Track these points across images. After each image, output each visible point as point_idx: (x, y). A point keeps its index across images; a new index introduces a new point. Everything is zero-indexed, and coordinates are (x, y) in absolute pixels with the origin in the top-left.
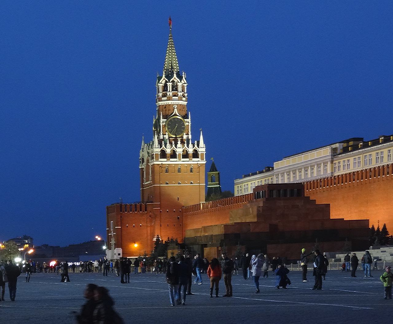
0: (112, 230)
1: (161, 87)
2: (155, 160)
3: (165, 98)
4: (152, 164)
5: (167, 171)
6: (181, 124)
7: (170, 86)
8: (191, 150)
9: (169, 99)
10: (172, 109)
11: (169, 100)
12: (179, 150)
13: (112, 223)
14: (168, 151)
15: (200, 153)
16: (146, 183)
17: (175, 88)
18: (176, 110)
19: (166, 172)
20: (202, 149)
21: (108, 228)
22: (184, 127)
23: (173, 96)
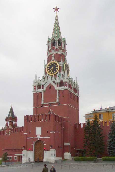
2: (67, 86)
3: (62, 50)
16: (44, 103)
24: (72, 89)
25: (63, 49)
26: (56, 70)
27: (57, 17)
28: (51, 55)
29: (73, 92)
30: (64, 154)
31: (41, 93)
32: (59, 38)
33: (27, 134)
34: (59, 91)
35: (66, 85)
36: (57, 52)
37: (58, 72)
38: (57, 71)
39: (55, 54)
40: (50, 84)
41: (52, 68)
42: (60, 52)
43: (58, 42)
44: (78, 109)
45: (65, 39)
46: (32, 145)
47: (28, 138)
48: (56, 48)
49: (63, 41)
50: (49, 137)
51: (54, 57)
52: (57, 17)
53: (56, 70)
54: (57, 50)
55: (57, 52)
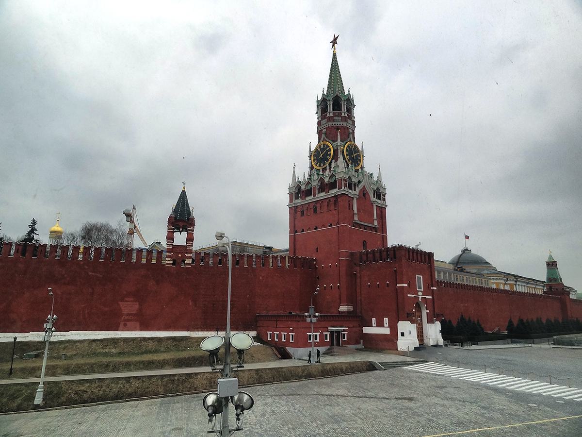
9: (345, 119)
25: (343, 115)
26: (328, 157)
27: (335, 55)
28: (321, 130)
32: (334, 96)
36: (330, 124)
37: (331, 162)
38: (330, 161)
39: (327, 129)
41: (321, 155)
42: (337, 122)
43: (331, 103)
45: (349, 94)
48: (328, 115)
49: (343, 99)
51: (326, 133)
52: (335, 55)
53: (328, 157)
54: (330, 119)
55: (330, 124)
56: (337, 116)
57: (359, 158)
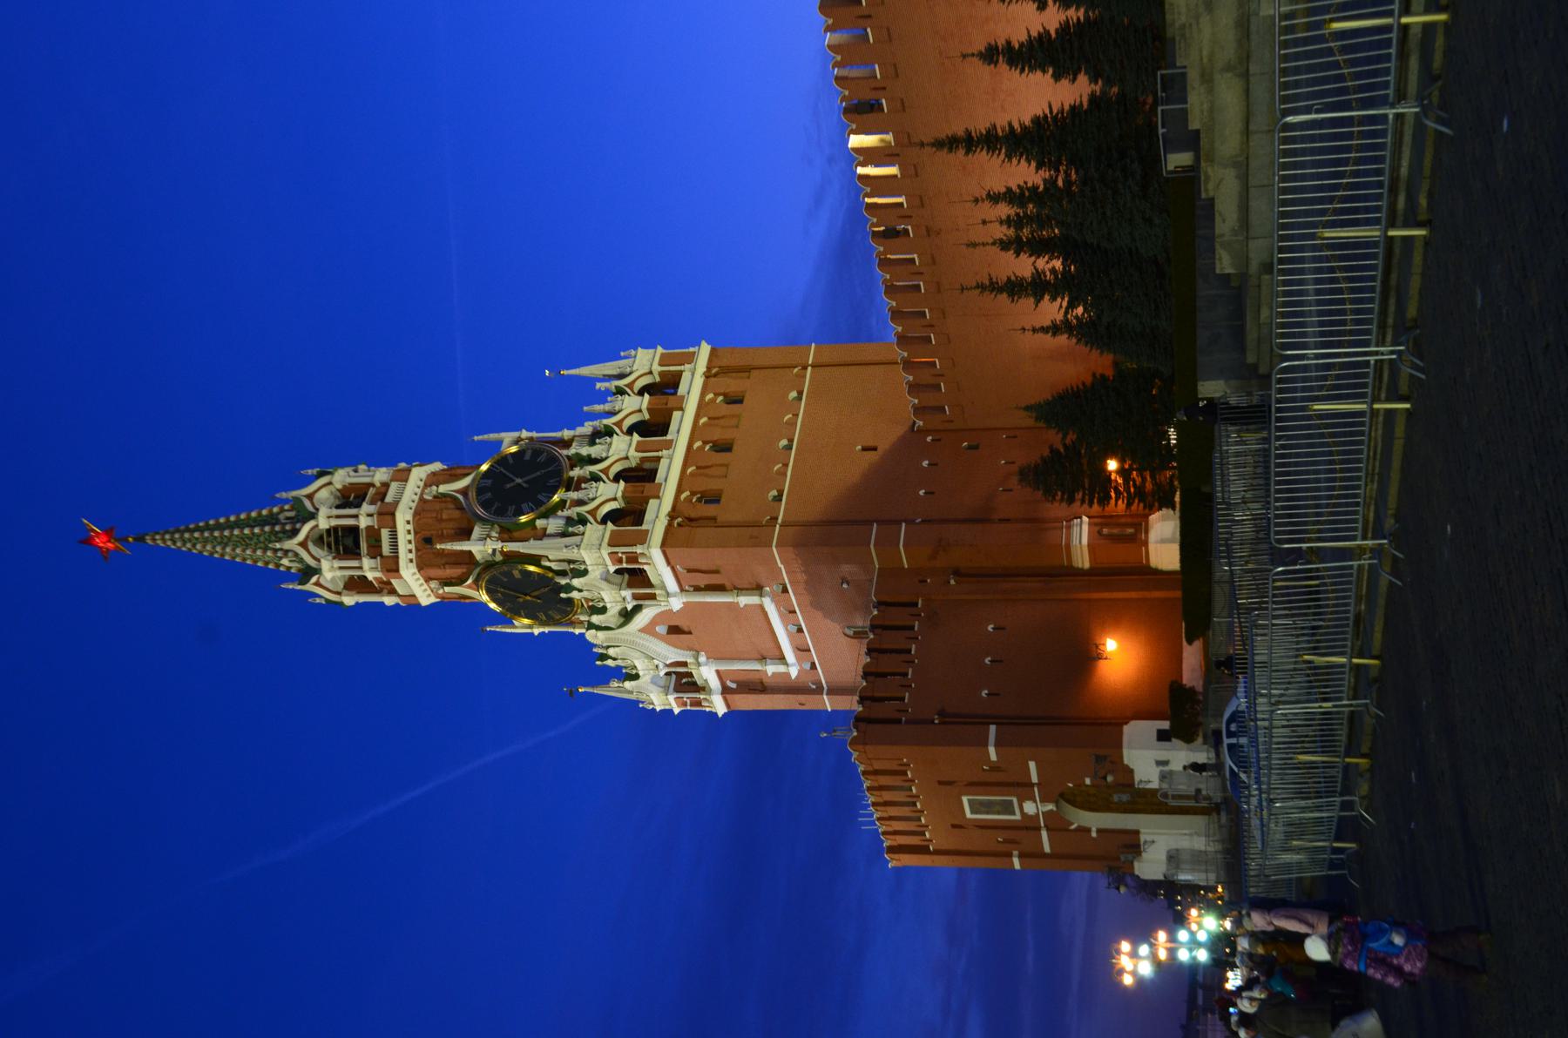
0: (1018, 817)
1: (337, 564)
2: (639, 549)
3: (385, 533)
4: (671, 584)
5: (712, 498)
6: (506, 465)
7: (338, 517)
8: (633, 407)
9: (387, 514)
10: (437, 506)
11: (393, 514)
12: (622, 449)
13: (975, 808)
14: (609, 494)
15: (657, 368)
17: (350, 498)
18: (443, 489)
19: (717, 501)
20: (645, 363)
21: (1010, 855)
22: (529, 453)
23: (382, 500)
24: (659, 459)
29: (683, 426)
30: (1157, 572)
31: (718, 672)
33: (1015, 853)
34: (682, 590)
35: (633, 558)
37: (549, 569)
40: (642, 630)
44: (805, 368)
46: (1094, 834)
47: (1047, 849)
48: (378, 575)
50: (1032, 765)
56: (379, 540)
57: (528, 457)
